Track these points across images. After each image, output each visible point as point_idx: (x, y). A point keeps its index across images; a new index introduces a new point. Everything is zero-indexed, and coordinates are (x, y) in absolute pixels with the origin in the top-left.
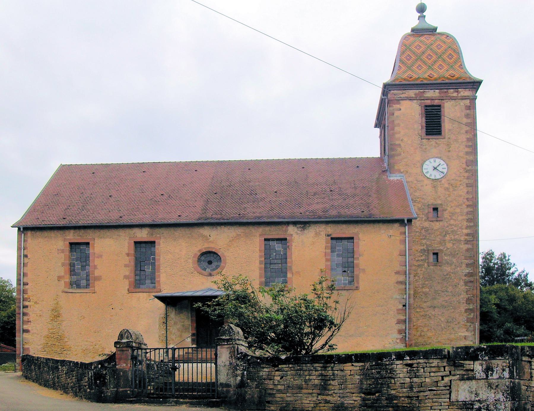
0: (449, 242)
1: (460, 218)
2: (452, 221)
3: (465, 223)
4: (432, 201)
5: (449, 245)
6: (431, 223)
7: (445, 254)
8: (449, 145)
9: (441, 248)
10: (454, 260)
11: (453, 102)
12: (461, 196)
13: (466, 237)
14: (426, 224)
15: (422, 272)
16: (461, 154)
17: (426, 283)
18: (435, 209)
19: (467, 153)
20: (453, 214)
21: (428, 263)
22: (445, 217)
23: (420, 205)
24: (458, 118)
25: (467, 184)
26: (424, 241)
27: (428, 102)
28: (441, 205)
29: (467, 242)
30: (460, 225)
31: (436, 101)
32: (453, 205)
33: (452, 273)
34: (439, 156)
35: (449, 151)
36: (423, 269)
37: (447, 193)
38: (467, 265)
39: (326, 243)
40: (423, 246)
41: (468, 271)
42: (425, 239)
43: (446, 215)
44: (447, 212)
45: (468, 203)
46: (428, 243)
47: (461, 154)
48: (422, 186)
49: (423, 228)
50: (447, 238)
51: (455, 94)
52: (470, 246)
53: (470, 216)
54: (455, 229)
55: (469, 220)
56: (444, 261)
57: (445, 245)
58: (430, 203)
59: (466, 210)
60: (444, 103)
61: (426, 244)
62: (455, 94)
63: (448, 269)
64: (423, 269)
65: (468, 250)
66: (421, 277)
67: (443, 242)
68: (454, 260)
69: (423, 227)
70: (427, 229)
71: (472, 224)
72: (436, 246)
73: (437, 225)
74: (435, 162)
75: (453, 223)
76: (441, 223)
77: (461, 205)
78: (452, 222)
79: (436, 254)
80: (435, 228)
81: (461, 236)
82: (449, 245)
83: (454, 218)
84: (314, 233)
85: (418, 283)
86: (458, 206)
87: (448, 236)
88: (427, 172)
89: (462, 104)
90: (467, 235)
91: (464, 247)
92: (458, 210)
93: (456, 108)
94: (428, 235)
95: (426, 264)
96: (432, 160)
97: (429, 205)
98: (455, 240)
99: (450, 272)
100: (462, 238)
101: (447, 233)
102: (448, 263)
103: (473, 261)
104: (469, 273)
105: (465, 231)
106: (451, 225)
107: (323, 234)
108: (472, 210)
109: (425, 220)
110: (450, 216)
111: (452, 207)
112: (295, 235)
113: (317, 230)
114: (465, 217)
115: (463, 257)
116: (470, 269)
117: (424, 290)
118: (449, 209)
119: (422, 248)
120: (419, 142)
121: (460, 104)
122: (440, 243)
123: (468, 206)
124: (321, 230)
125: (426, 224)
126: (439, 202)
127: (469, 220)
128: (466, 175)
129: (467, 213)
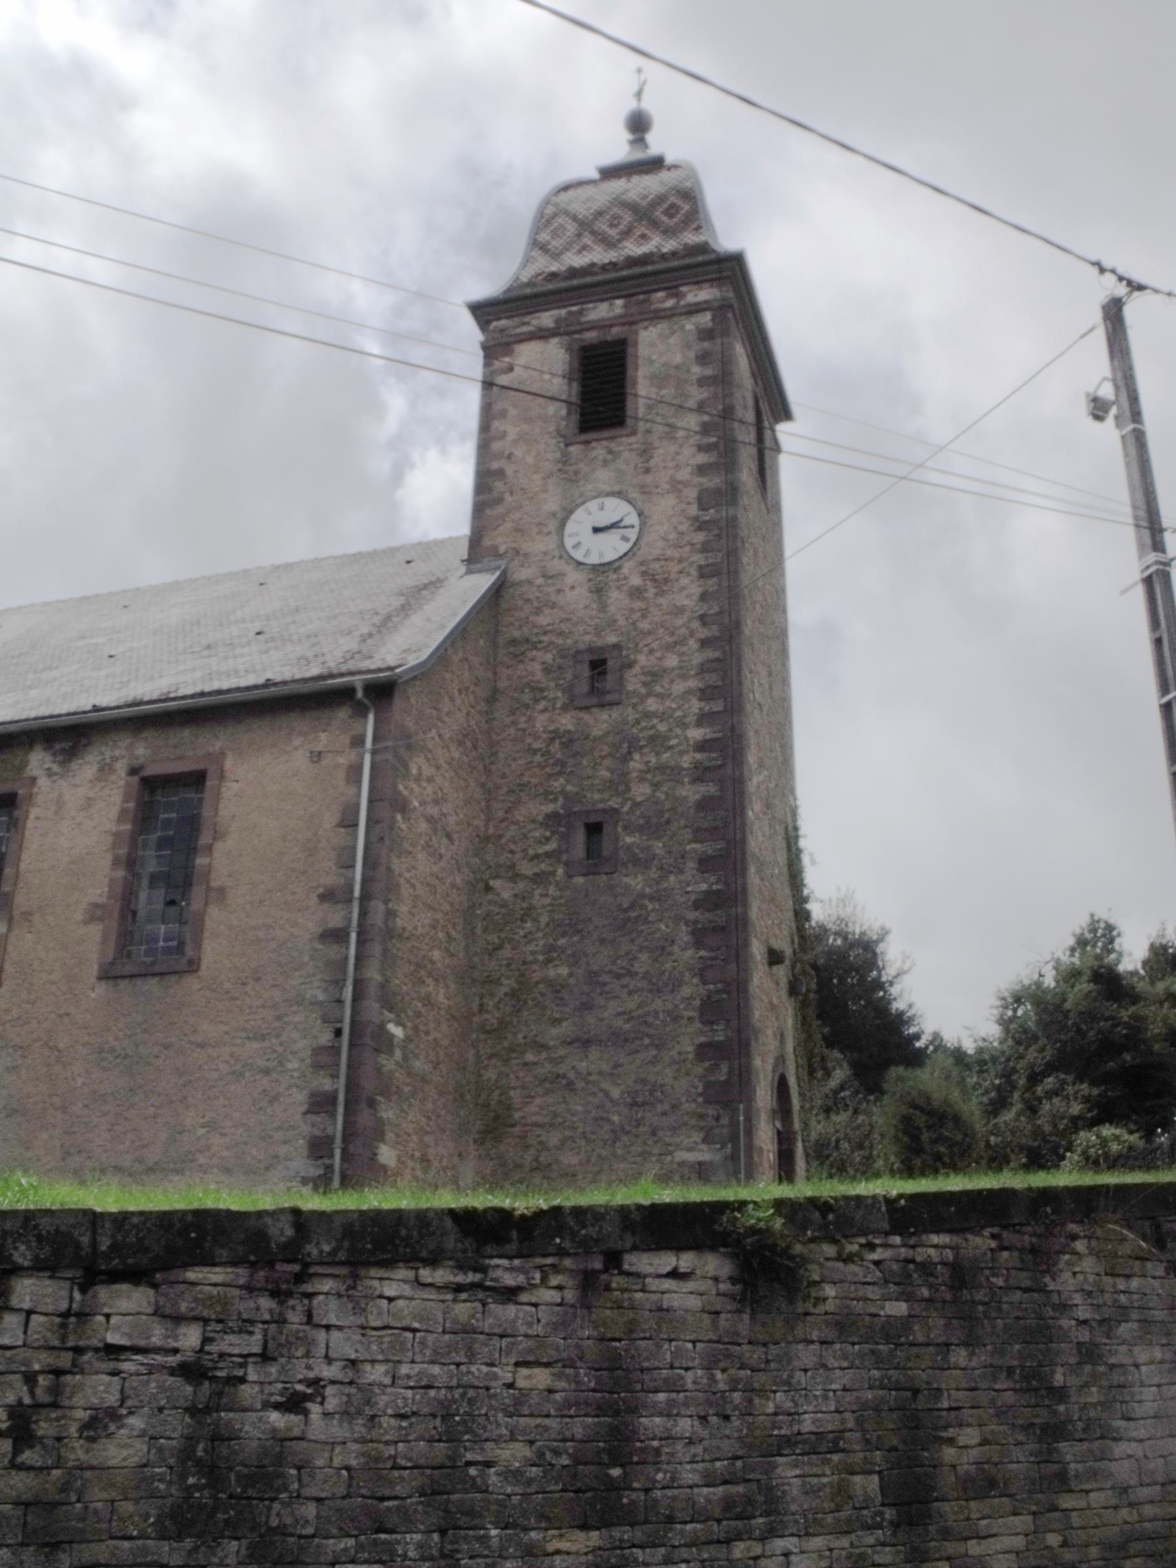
0: (641, 780)
1: (679, 688)
2: (650, 701)
3: (695, 705)
4: (587, 638)
5: (640, 791)
6: (581, 714)
7: (625, 828)
8: (646, 452)
9: (614, 803)
10: (658, 847)
11: (662, 326)
12: (681, 610)
13: (698, 756)
14: (567, 722)
15: (547, 901)
16: (684, 474)
17: (562, 942)
18: (598, 666)
19: (701, 470)
20: (654, 675)
21: (567, 864)
22: (630, 688)
23: (549, 657)
24: (677, 367)
25: (700, 567)
26: (557, 784)
27: (591, 336)
28: (617, 647)
29: (700, 774)
30: (679, 713)
31: (615, 330)
32: (655, 645)
33: (651, 898)
34: (617, 488)
35: (647, 471)
36: (552, 890)
37: (638, 604)
38: (705, 864)
39: (126, 800)
40: (555, 800)
41: (704, 887)
42: (560, 773)
43: (633, 682)
44: (636, 669)
45: (703, 633)
46: (569, 788)
47: (684, 474)
48: (559, 591)
49: (555, 735)
50: (636, 764)
51: (670, 303)
52: (711, 789)
53: (713, 679)
54: (662, 728)
55: (705, 694)
56: (622, 855)
57: (629, 789)
58: (581, 646)
59: (697, 659)
60: (636, 333)
61: (563, 792)
62: (670, 303)
63: (636, 882)
64: (552, 890)
65: (704, 804)
66: (544, 919)
67: (619, 783)
68: (658, 847)
69: (556, 731)
70: (568, 741)
71: (718, 706)
72: (597, 796)
73: (601, 722)
74: (602, 508)
75: (653, 708)
76: (615, 713)
77: (682, 642)
78: (652, 704)
79: (594, 829)
80: (596, 732)
81: (682, 753)
82: (640, 791)
83: (658, 689)
84: (95, 769)
85: (529, 948)
86: (669, 647)
87: (637, 756)
88: (577, 545)
89: (689, 327)
90: (703, 746)
91: (691, 793)
92: (672, 661)
93: (672, 341)
94: (571, 761)
95: (560, 871)
96: (593, 505)
97: (577, 652)
98: (661, 768)
99: (642, 896)
100: (686, 761)
101: (634, 746)
102: (635, 861)
103: (721, 845)
104: (708, 893)
105: (696, 734)
106: (648, 715)
107: (121, 768)
108: (717, 654)
109: (565, 708)
110: (645, 684)
111: (651, 652)
112: (43, 782)
113: (108, 754)
114: (693, 683)
115: (688, 834)
116: (713, 879)
117: (552, 973)
118: (642, 659)
119: (550, 808)
120: (558, 455)
121: (682, 328)
122: (611, 785)
123: (704, 643)
124: (117, 753)
125: (567, 722)
126: (612, 639)
127: (705, 694)
128: (700, 537)
129: (703, 669)
